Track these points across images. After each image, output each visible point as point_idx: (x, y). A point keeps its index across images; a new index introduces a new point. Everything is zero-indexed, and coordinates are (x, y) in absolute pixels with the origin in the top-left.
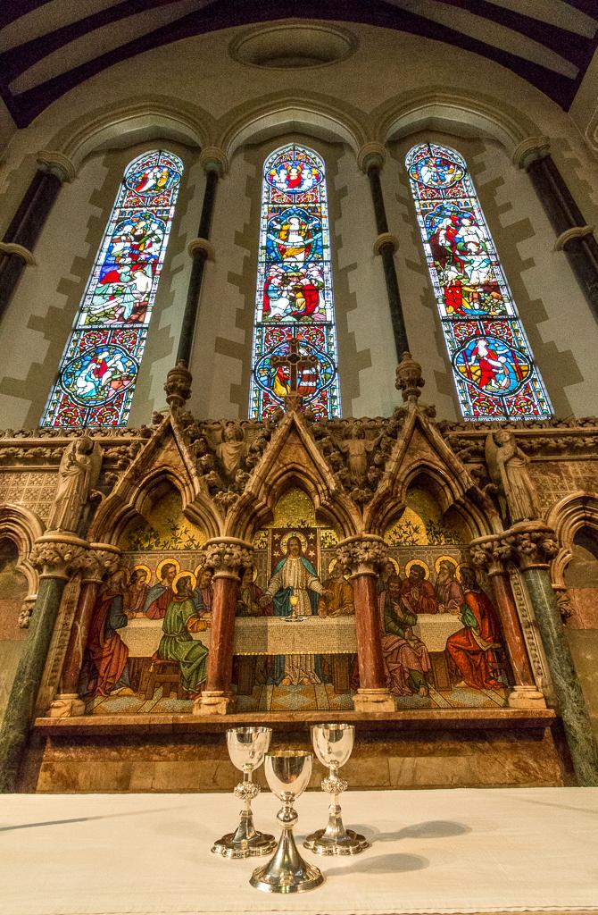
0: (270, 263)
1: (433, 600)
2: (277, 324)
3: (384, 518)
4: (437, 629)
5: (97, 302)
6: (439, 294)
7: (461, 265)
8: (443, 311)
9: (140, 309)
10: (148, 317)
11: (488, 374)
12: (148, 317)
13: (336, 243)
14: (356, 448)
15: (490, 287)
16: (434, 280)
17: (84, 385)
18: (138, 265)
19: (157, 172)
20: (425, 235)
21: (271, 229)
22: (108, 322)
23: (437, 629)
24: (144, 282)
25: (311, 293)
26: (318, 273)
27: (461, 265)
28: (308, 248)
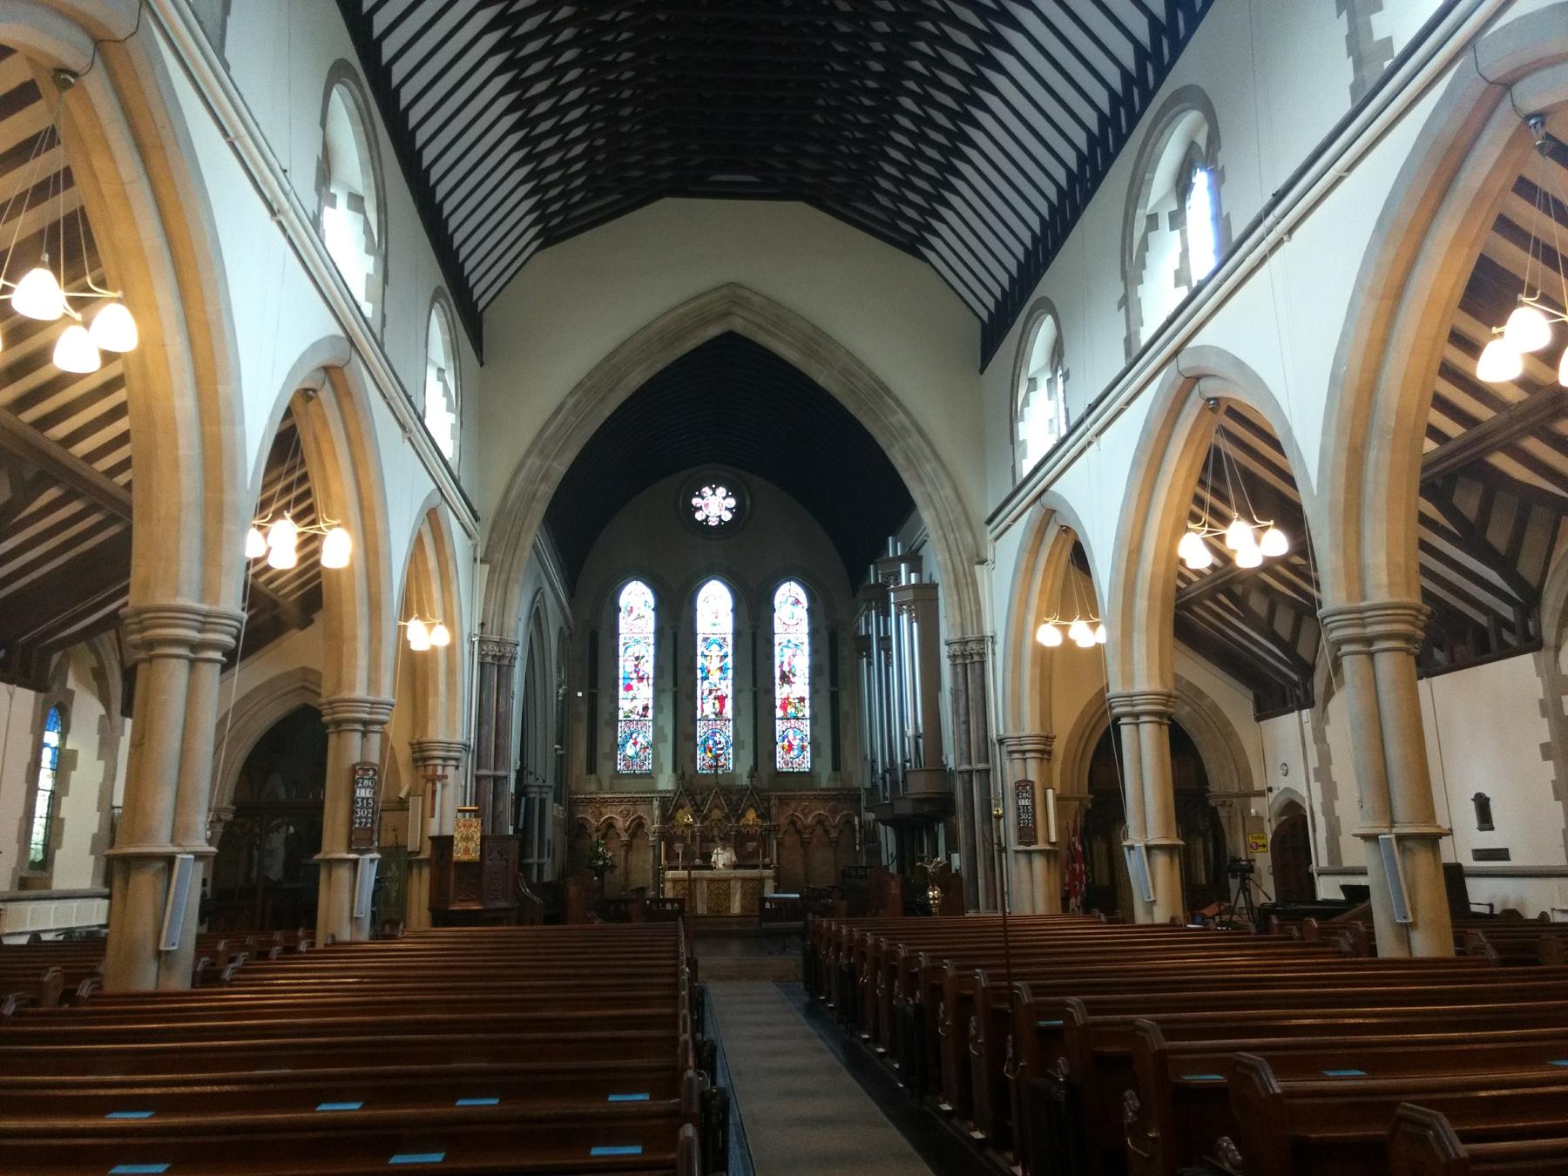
0: (704, 679)
1: (752, 838)
2: (706, 718)
3: (743, 815)
4: (751, 846)
5: (625, 705)
6: (778, 703)
7: (789, 682)
8: (779, 713)
9: (646, 708)
10: (650, 713)
11: (791, 746)
12: (650, 713)
13: (735, 668)
14: (734, 798)
15: (802, 700)
16: (778, 695)
17: (630, 750)
18: (641, 679)
19: (637, 602)
20: (777, 664)
21: (704, 655)
22: (633, 717)
23: (751, 846)
24: (644, 693)
25: (721, 699)
26: (727, 688)
27: (789, 682)
28: (721, 669)
